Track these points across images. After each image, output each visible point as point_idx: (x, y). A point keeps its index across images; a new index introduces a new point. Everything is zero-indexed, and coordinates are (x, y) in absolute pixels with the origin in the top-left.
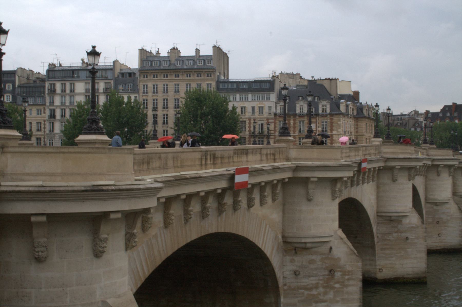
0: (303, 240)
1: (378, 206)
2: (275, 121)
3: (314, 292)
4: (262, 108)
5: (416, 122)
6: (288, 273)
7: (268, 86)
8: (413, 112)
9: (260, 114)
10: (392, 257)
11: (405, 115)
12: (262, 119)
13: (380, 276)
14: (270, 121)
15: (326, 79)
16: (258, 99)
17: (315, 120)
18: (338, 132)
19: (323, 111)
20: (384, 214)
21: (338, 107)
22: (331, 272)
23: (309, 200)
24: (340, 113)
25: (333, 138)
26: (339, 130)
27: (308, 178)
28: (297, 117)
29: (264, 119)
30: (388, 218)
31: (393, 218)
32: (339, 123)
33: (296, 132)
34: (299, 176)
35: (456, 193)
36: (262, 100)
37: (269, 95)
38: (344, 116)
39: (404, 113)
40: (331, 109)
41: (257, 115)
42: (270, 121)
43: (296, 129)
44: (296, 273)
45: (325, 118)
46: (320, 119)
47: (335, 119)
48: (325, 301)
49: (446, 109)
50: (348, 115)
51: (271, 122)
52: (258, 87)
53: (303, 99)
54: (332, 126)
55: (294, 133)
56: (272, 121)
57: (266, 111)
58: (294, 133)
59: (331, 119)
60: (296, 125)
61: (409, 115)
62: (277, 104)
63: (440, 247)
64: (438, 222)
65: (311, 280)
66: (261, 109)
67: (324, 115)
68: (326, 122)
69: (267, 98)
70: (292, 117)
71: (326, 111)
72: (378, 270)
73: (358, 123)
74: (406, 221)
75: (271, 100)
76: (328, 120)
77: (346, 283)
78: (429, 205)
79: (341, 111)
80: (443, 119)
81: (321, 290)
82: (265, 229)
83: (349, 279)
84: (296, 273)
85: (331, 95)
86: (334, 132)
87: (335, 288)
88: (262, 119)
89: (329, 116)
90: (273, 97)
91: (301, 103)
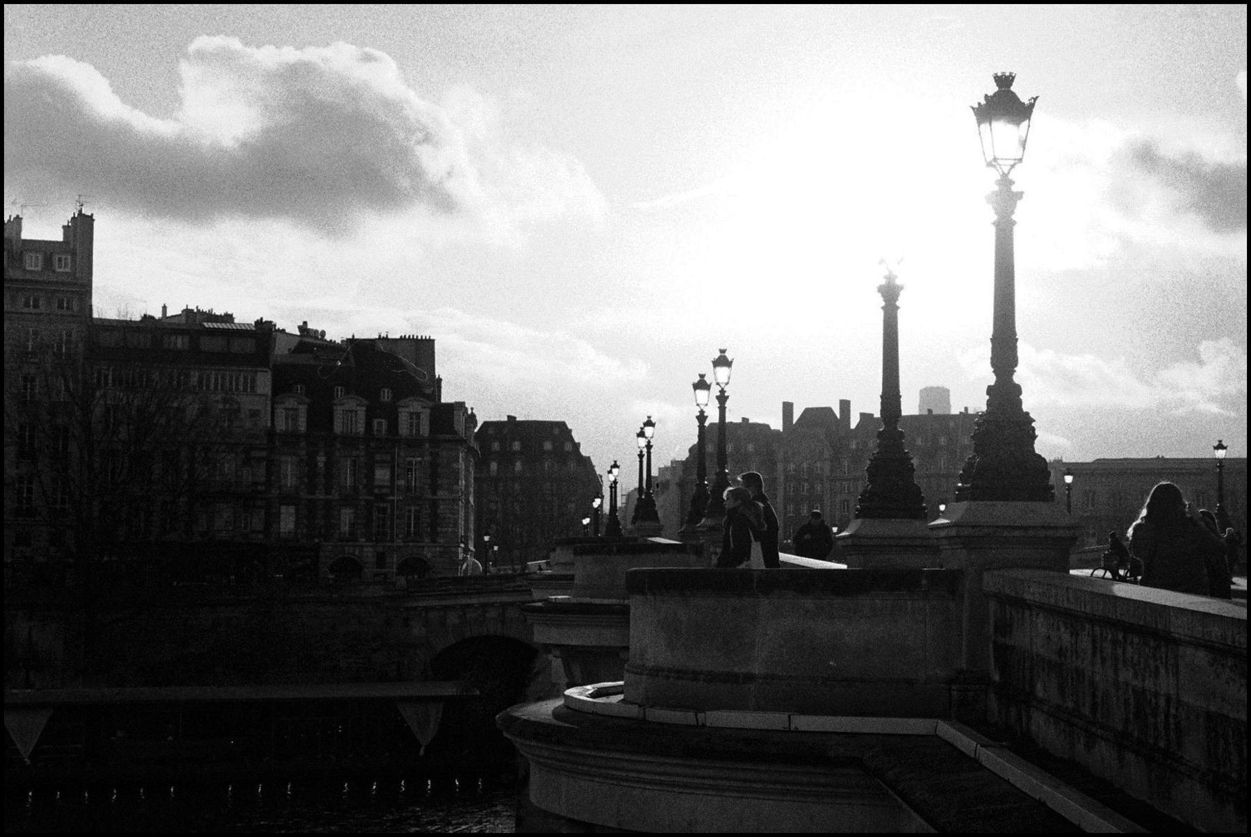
7: (250, 346)
14: (255, 454)
17: (388, 458)
25: (439, 511)
26: (455, 487)
28: (339, 446)
32: (455, 465)
33: (333, 491)
42: (255, 454)
51: (259, 460)
53: (348, 393)
55: (328, 492)
56: (264, 454)
58: (328, 492)
62: (277, 403)
67: (414, 443)
71: (418, 430)
79: (456, 433)
86: (441, 494)
90: (264, 382)
91: (351, 404)
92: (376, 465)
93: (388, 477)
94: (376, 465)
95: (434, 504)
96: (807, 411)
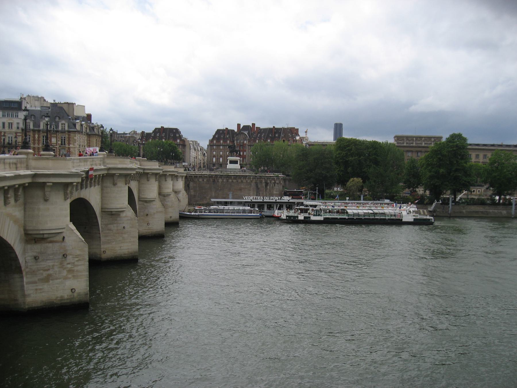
0: (41, 232)
1: (102, 204)
2: (22, 135)
3: (51, 272)
4: (12, 124)
5: (135, 140)
6: (29, 258)
7: (16, 106)
8: (133, 132)
9: (9, 128)
10: (113, 242)
11: (127, 134)
12: (11, 133)
13: (104, 256)
14: (18, 134)
15: (65, 103)
16: (8, 115)
17: (56, 136)
18: (74, 145)
19: (62, 129)
20: (107, 210)
21: (75, 125)
22: (65, 256)
23: (46, 200)
24: (75, 130)
26: (75, 144)
27: (44, 184)
29: (13, 133)
30: (110, 213)
31: (113, 213)
32: (75, 138)
34: (38, 181)
35: (161, 193)
36: (11, 116)
37: (18, 114)
38: (79, 133)
39: (126, 133)
40: (68, 126)
41: (7, 129)
42: (18, 134)
43: (40, 142)
44: (36, 258)
45: (64, 134)
46: (60, 135)
47: (72, 135)
48: (59, 279)
49: (156, 131)
50: (82, 132)
51: (19, 136)
52: (8, 106)
54: (69, 140)
55: (39, 145)
57: (15, 126)
58: (39, 145)
59: (69, 135)
60: (40, 139)
61: (129, 134)
63: (149, 233)
64: (147, 215)
65: (48, 263)
66: (11, 125)
67: (63, 132)
68: (64, 137)
69: (15, 116)
70: (37, 132)
72: (102, 252)
73: (91, 139)
74: (123, 215)
75: (19, 117)
76: (67, 136)
77: (76, 263)
78: (141, 203)
80: (154, 138)
81: (56, 269)
82: (9, 225)
83: (77, 261)
84: (36, 258)
85: (68, 116)
86: (71, 146)
87: (68, 268)
88: (11, 133)
89: (67, 132)
92: (52, 138)
93: (55, 141)
94: (52, 138)
95: (69, 148)
96: (244, 127)
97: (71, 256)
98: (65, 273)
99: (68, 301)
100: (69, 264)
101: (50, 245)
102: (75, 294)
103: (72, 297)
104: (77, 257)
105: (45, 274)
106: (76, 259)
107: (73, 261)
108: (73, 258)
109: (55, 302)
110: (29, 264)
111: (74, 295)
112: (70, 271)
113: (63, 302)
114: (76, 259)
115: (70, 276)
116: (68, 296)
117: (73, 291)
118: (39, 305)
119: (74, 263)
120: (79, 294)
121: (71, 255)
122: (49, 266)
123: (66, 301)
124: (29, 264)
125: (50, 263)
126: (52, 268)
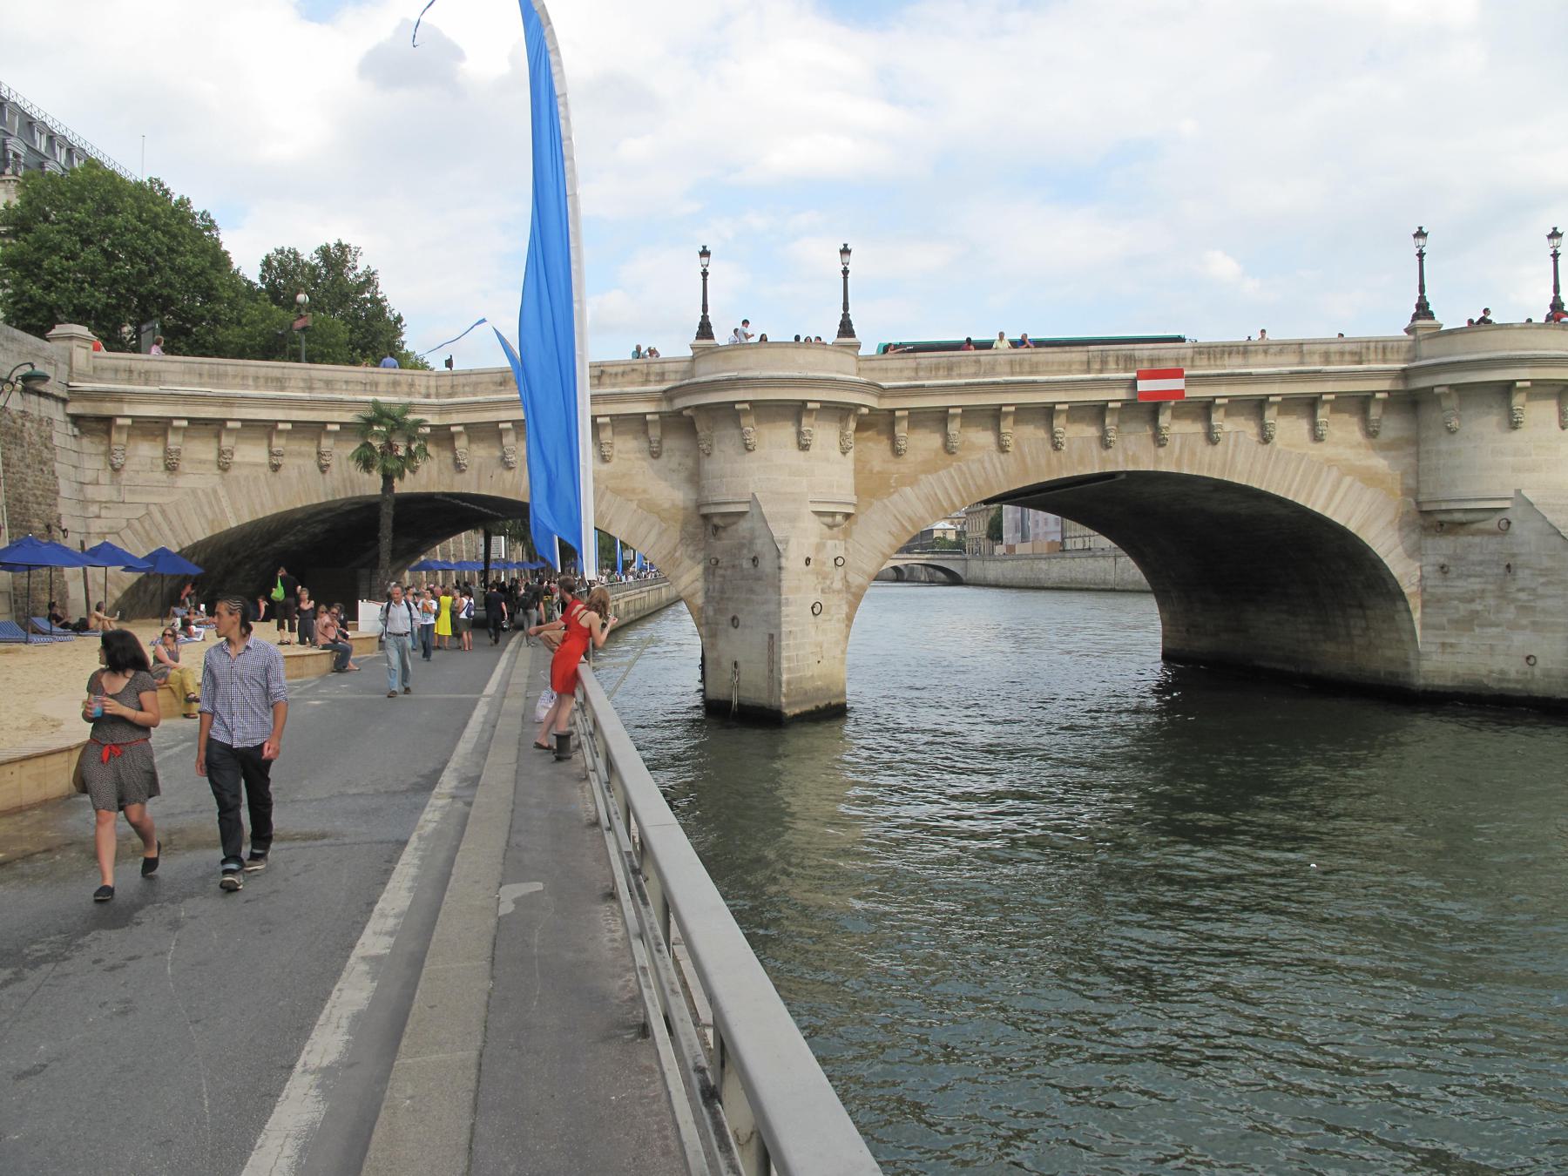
0: (1444, 506)
3: (1477, 606)
6: (1430, 568)
44: (1443, 568)
48: (1497, 626)
77: (1540, 590)
81: (1492, 602)
83: (1543, 584)
84: (1443, 568)
87: (1519, 600)
97: (1527, 572)
98: (1510, 613)
99: (1519, 686)
100: (1521, 590)
101: (1477, 539)
102: (1537, 671)
103: (1529, 677)
104: (1546, 575)
105: (1463, 609)
106: (1542, 580)
107: (1533, 586)
108: (1533, 575)
109: (1486, 681)
110: (1429, 583)
111: (1533, 674)
112: (1524, 609)
113: (1505, 685)
114: (1542, 580)
115: (1524, 622)
116: (1517, 672)
117: (1532, 661)
118: (1450, 684)
119: (1534, 590)
120: (1547, 674)
121: (1527, 568)
122: (1473, 591)
123: (1512, 686)
124: (1429, 583)
125: (1475, 584)
126: (1480, 598)
